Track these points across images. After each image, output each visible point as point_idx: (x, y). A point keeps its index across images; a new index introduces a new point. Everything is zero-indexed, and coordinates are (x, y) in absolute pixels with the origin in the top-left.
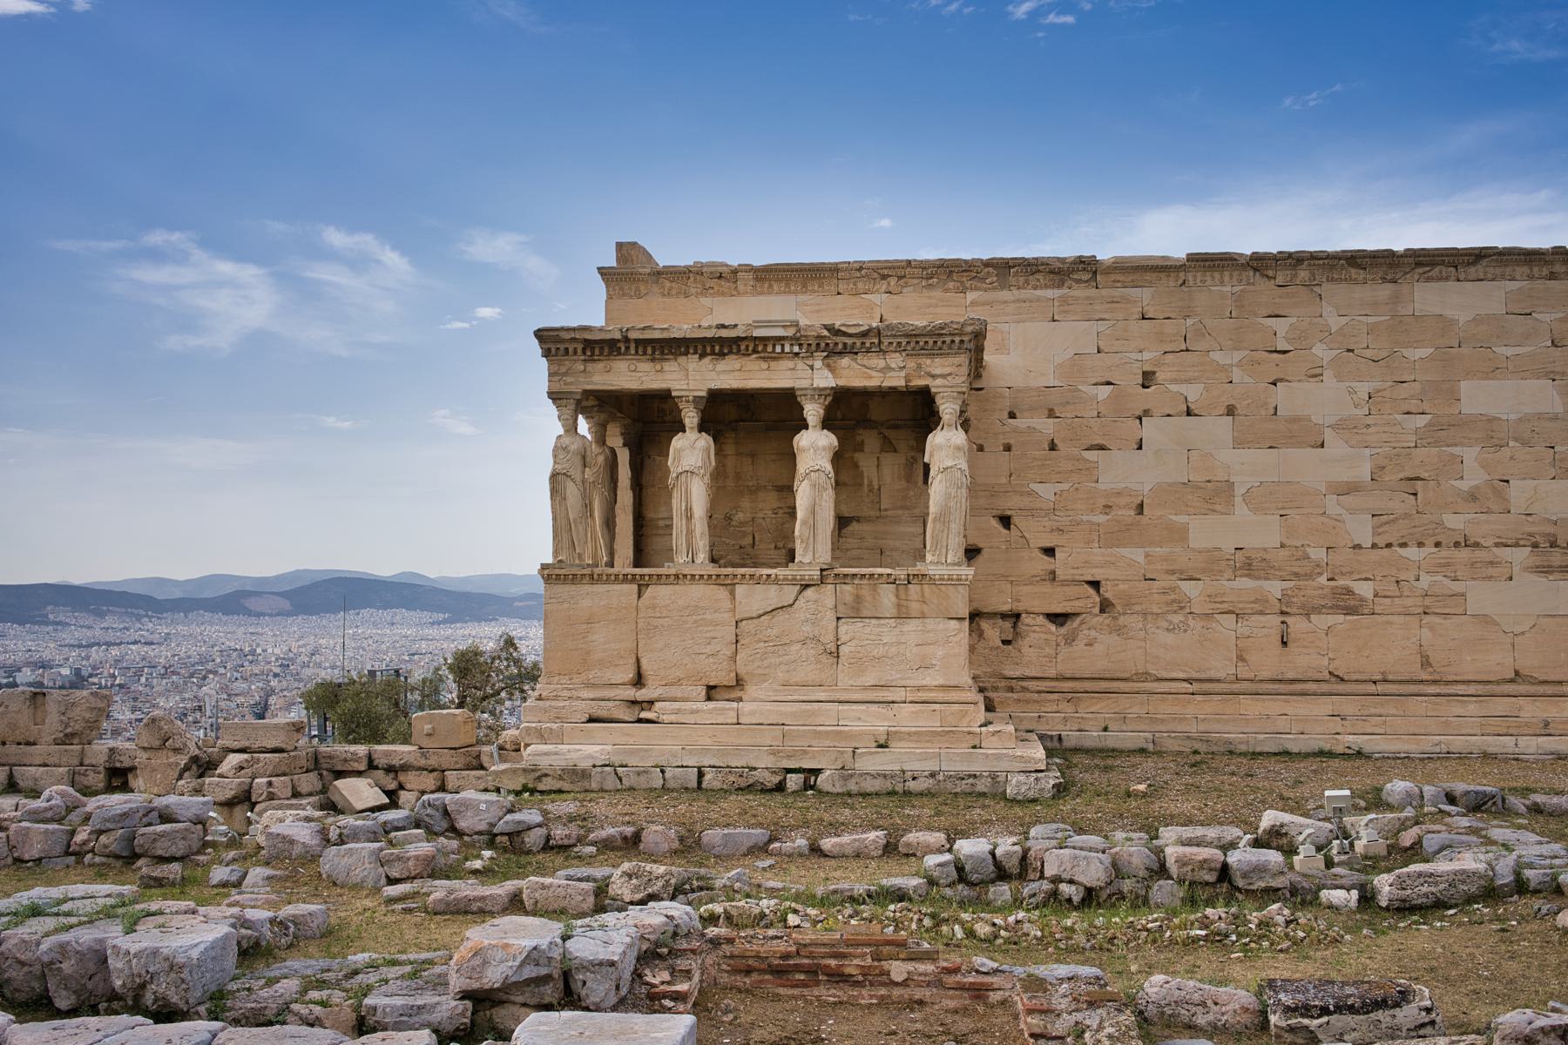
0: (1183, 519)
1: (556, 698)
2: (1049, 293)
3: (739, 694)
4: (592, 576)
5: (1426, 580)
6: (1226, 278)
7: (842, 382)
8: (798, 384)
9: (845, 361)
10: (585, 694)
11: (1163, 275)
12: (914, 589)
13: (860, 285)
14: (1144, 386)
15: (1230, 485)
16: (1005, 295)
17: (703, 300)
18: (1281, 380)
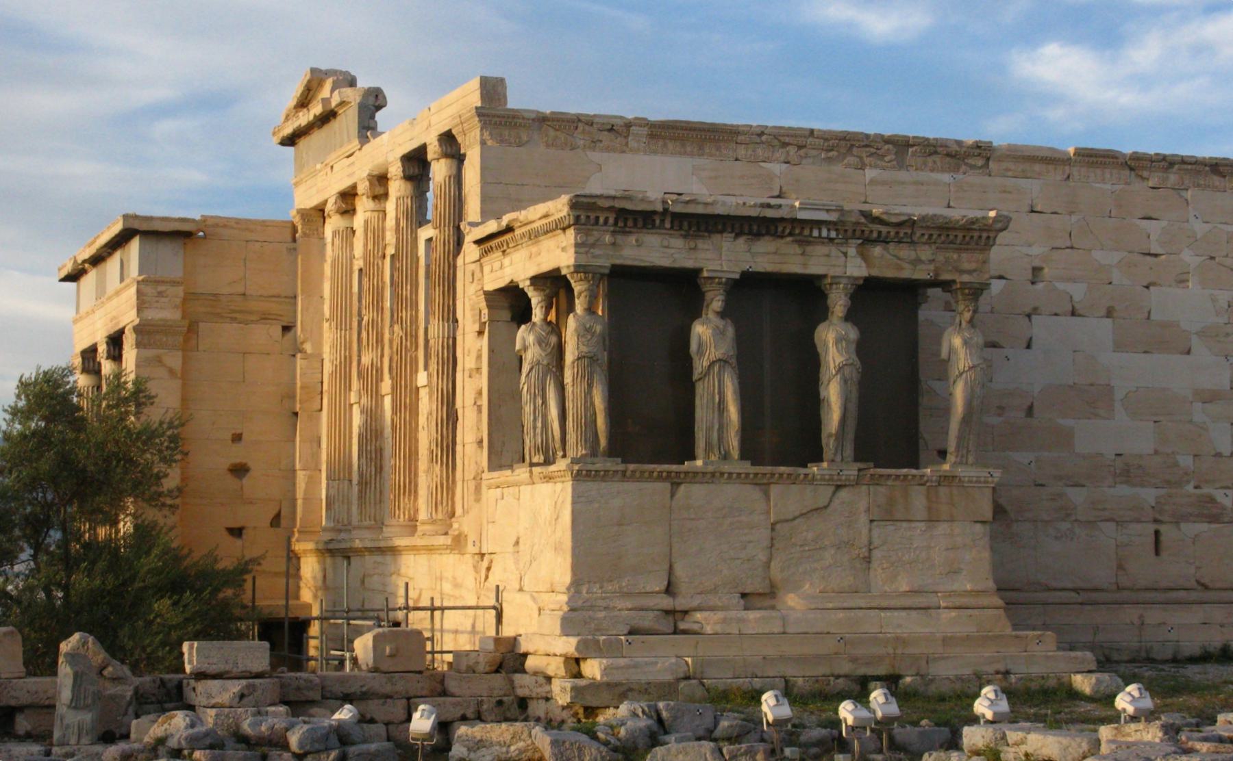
0: (1069, 422)
1: (592, 608)
2: (946, 177)
3: (771, 602)
4: (624, 472)
6: (1107, 176)
7: (875, 272)
8: (832, 272)
9: (877, 250)
10: (620, 603)
11: (1050, 167)
12: (943, 491)
13: (760, 151)
14: (1033, 283)
15: (1109, 389)
16: (902, 175)
17: (590, 154)
18: (1154, 284)
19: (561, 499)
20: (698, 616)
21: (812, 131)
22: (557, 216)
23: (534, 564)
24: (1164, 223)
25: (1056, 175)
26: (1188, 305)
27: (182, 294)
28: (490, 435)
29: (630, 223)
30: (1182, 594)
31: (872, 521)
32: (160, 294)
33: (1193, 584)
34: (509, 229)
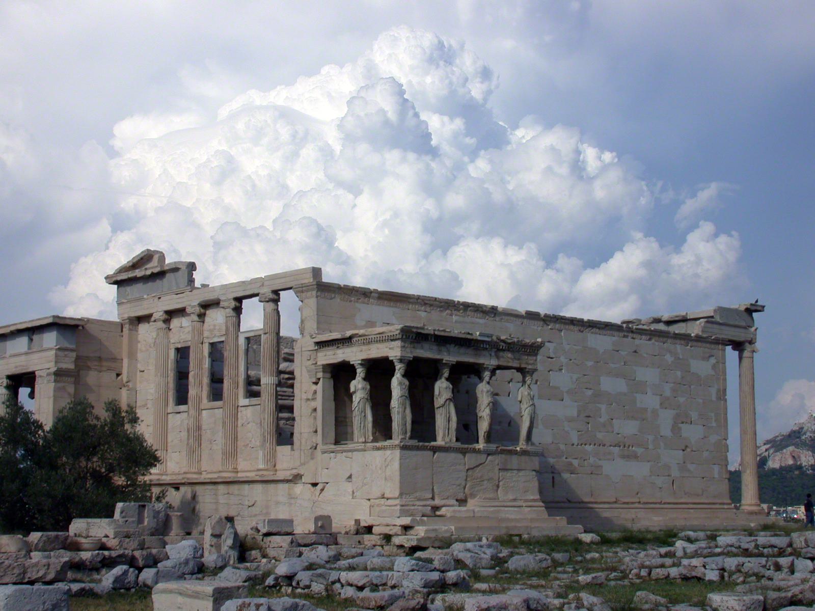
2: (481, 321)
5: (592, 460)
10: (418, 503)
18: (551, 370)
19: (389, 458)
20: (444, 509)
21: (436, 298)
22: (389, 334)
24: (554, 345)
25: (519, 321)
26: (562, 380)
27: (75, 356)
29: (420, 338)
30: (562, 504)
31: (500, 469)
32: (66, 356)
33: (565, 500)
34: (350, 339)
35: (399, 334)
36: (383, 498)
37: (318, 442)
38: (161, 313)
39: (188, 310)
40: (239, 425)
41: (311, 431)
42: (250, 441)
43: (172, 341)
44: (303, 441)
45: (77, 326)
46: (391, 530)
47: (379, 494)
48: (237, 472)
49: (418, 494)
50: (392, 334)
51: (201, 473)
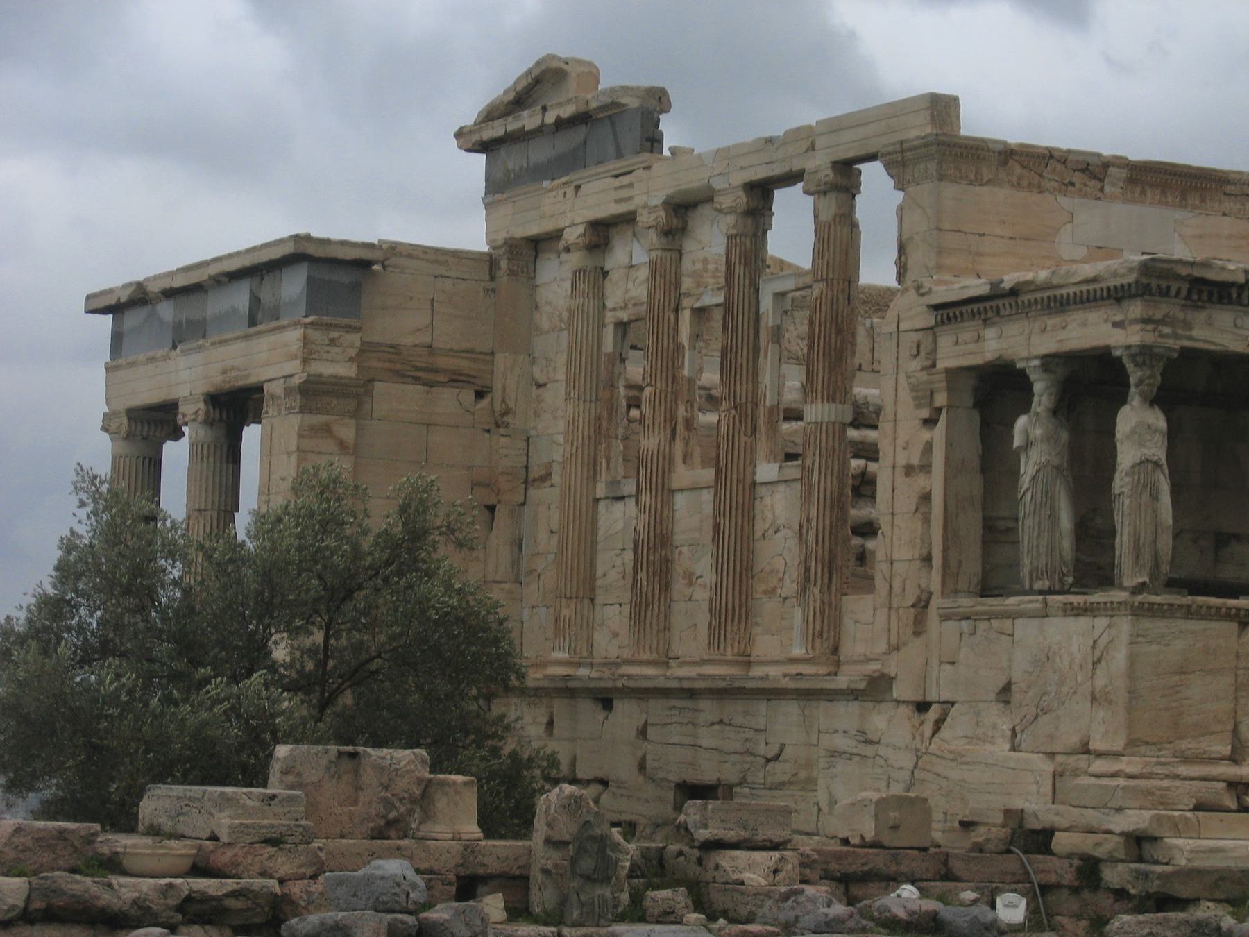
4: (1189, 606)
10: (1183, 770)
17: (1061, 198)
22: (1112, 283)
23: (1044, 719)
27: (358, 344)
28: (945, 550)
29: (1205, 297)
32: (333, 342)
34: (1014, 292)
35: (1137, 282)
36: (1088, 752)
37: (932, 588)
38: (580, 229)
39: (644, 218)
40: (758, 535)
41: (917, 556)
42: (782, 580)
43: (609, 304)
44: (897, 585)
45: (363, 265)
46: (1098, 844)
47: (1074, 740)
48: (749, 664)
49: (1184, 745)
50: (1118, 282)
51: (667, 666)
